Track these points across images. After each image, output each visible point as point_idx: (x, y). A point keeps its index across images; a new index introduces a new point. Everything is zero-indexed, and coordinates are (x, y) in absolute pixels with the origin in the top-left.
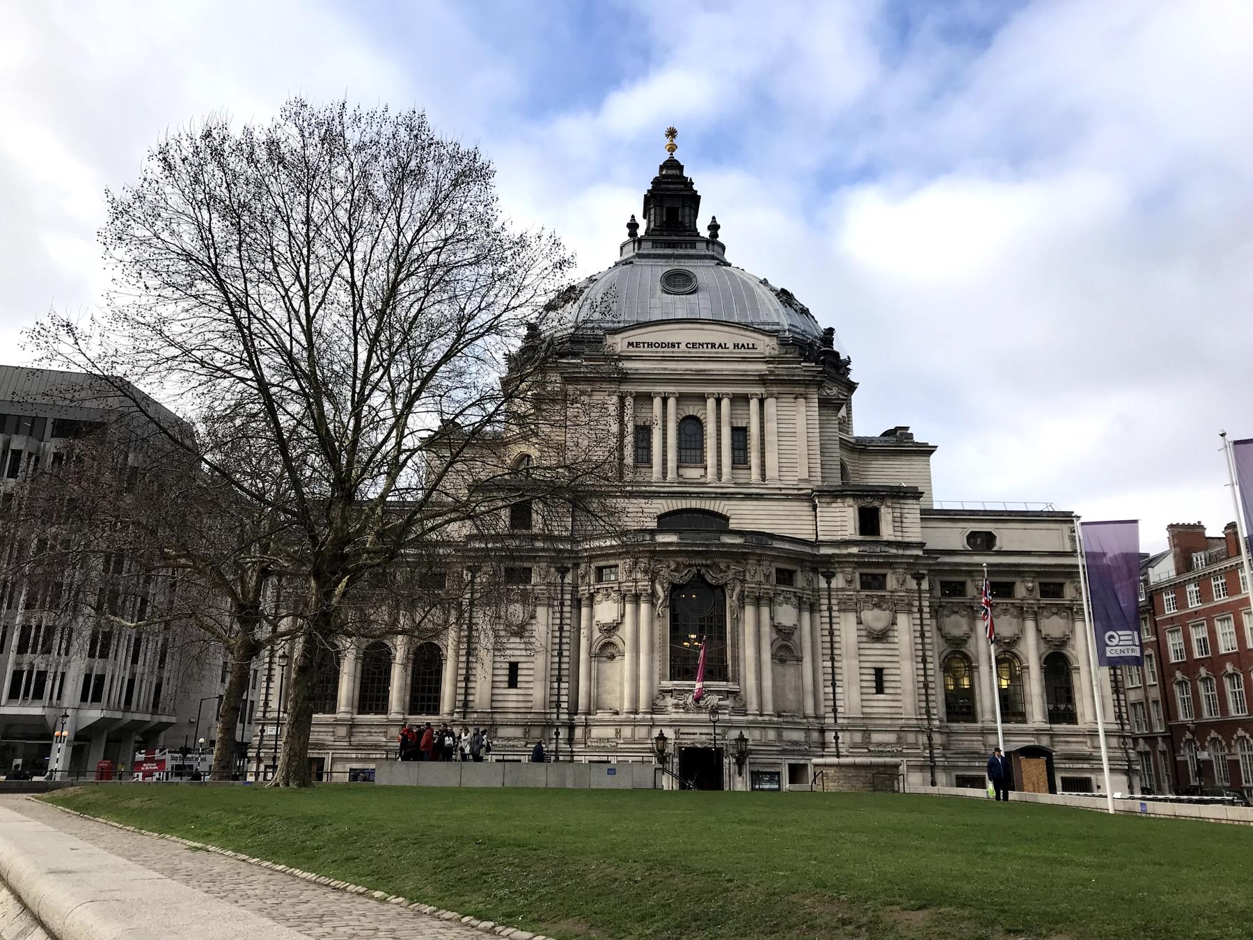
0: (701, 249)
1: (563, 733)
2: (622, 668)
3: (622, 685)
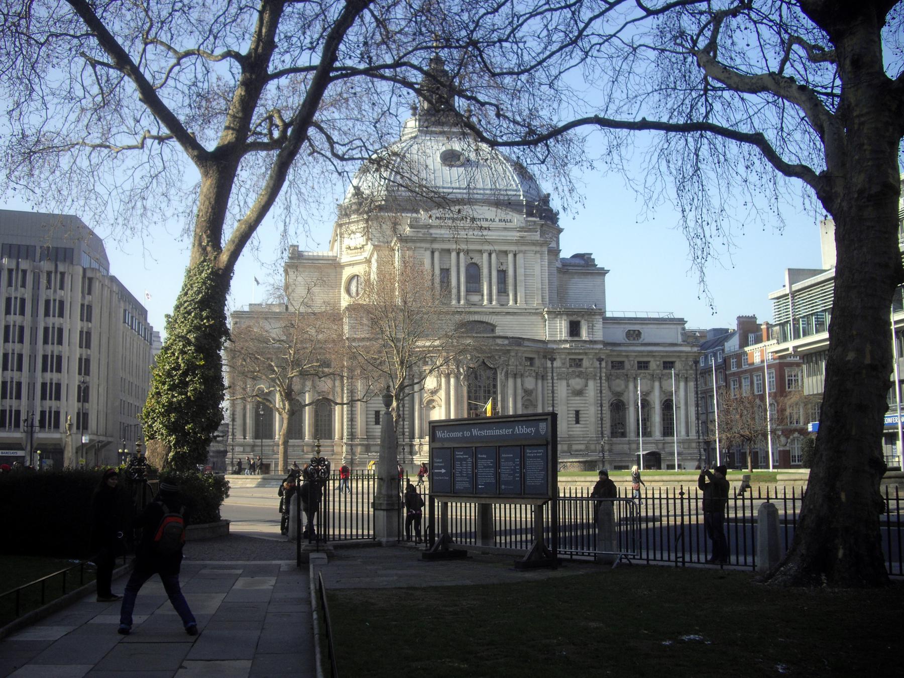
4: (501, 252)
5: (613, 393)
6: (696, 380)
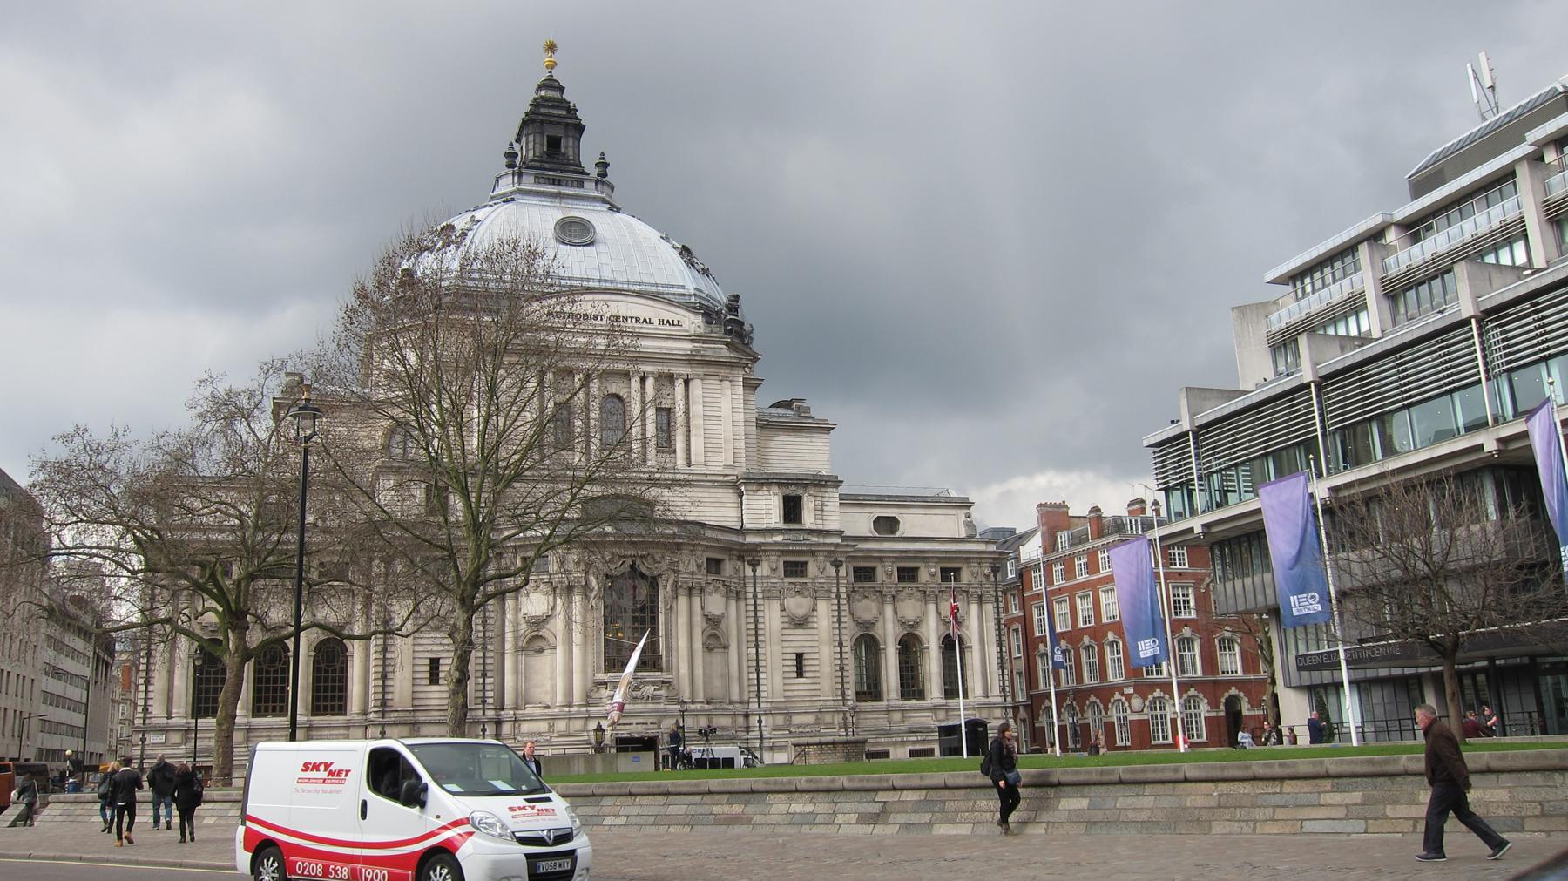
0: (589, 189)
1: (490, 729)
2: (554, 661)
3: (553, 678)
4: (660, 375)
5: (858, 624)
6: (997, 601)
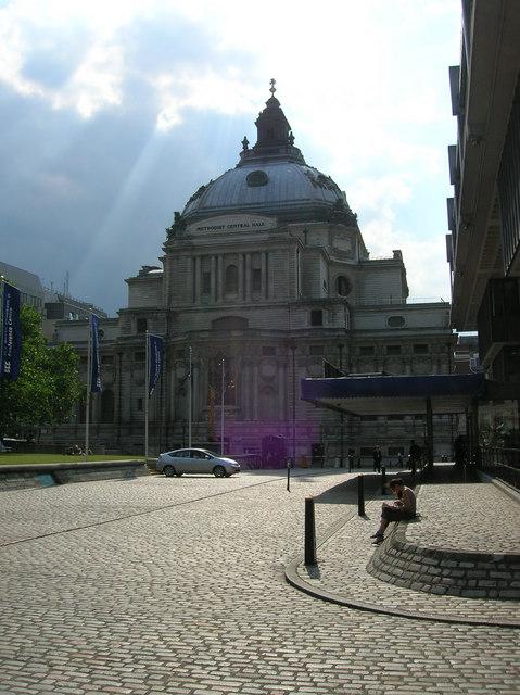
4: (254, 253)
